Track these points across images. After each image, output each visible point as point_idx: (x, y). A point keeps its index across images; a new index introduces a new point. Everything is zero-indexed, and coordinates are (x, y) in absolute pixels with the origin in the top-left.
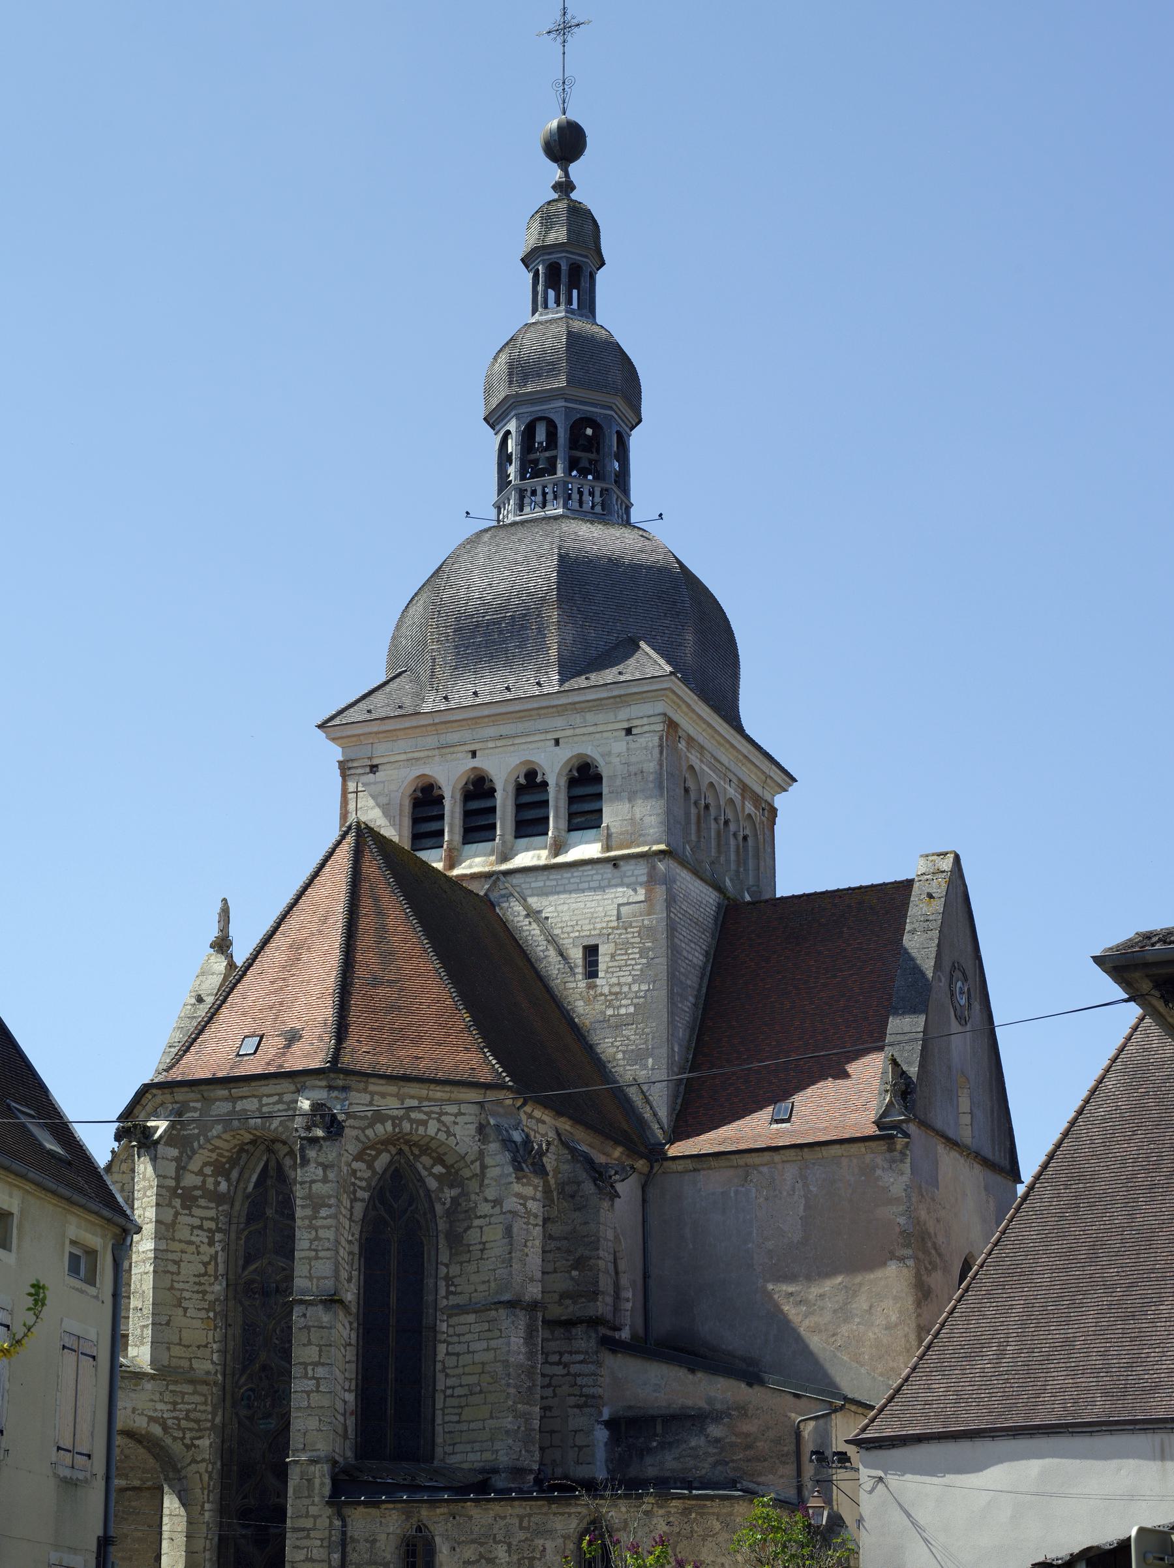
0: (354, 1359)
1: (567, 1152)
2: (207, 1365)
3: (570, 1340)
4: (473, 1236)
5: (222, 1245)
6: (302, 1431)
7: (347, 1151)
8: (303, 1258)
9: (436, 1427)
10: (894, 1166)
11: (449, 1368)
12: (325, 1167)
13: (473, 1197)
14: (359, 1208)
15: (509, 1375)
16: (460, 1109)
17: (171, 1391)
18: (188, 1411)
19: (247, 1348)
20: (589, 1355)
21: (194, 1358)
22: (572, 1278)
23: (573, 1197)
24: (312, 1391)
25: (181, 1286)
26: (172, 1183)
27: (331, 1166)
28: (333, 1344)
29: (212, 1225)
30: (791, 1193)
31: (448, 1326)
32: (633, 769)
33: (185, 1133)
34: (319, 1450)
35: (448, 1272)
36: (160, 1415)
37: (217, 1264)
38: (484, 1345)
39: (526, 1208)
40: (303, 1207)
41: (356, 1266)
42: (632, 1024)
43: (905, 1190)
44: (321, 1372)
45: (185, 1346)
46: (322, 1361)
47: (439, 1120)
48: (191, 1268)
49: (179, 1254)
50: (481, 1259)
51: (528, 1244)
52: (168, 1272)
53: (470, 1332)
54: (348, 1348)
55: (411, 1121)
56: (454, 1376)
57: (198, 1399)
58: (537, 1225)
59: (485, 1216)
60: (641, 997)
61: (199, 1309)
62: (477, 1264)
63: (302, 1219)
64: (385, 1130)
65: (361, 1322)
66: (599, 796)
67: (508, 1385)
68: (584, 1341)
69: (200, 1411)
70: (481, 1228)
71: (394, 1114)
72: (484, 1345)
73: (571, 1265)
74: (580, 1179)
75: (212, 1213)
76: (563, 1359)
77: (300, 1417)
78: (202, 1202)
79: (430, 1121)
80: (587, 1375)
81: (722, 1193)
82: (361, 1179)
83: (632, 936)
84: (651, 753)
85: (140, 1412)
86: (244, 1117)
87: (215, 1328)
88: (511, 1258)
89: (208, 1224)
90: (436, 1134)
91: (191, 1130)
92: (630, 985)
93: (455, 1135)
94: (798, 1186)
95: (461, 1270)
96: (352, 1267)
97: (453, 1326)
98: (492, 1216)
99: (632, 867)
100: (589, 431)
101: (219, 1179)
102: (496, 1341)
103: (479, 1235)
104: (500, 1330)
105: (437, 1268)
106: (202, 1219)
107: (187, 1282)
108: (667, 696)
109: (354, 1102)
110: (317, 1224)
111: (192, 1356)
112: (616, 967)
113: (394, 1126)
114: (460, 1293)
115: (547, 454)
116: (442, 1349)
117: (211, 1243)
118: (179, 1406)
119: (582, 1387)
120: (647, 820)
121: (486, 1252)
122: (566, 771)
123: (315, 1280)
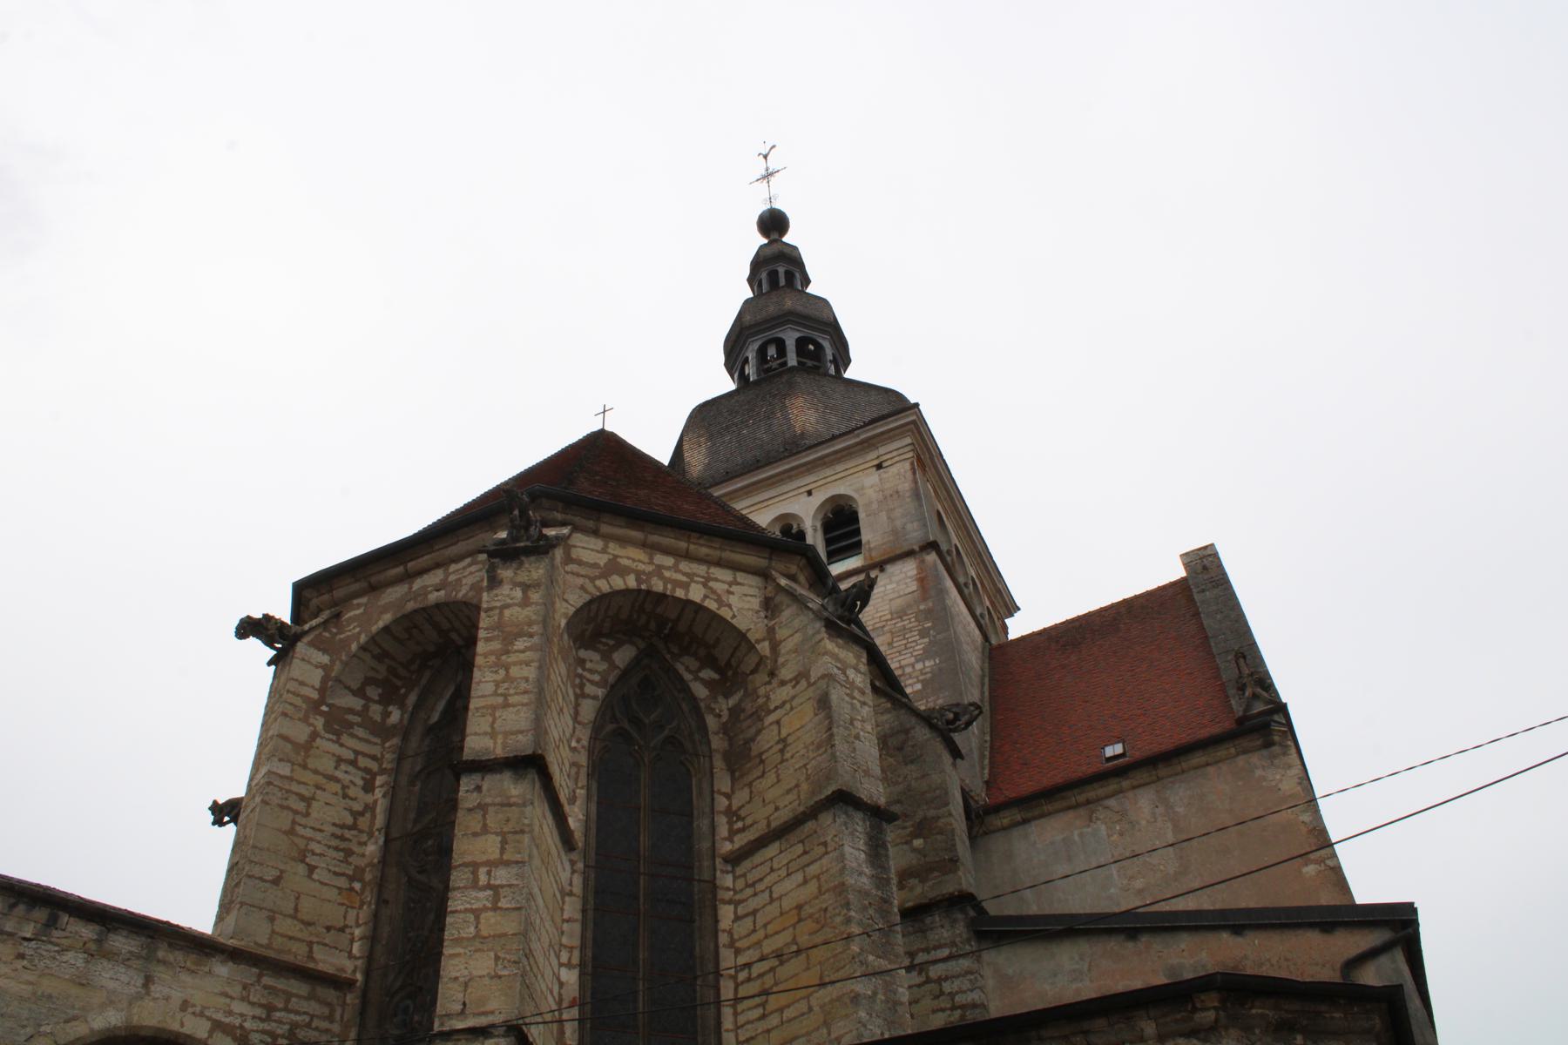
0: (578, 916)
1: (883, 700)
2: (344, 959)
3: (923, 931)
4: (767, 740)
5: (383, 790)
6: (461, 979)
7: (566, 601)
8: (483, 707)
9: (725, 1035)
10: (1276, 762)
11: (740, 939)
12: (526, 588)
13: (762, 691)
14: (588, 710)
15: (847, 905)
16: (735, 578)
17: (265, 987)
18: (294, 1026)
19: (411, 935)
20: (956, 946)
21: (318, 943)
22: (914, 850)
23: (900, 749)
24: (485, 909)
25: (308, 833)
26: (315, 695)
27: (537, 585)
28: (527, 829)
29: (374, 766)
30: (1153, 820)
31: (735, 879)
32: (888, 493)
33: (342, 636)
34: (492, 1012)
35: (730, 805)
36: (237, 1022)
37: (374, 817)
38: (799, 877)
39: (848, 677)
40: (487, 640)
41: (583, 781)
42: (922, 699)
43: (1300, 784)
44: (502, 876)
45: (303, 922)
46: (505, 857)
47: (705, 585)
48: (328, 812)
49: (312, 790)
50: (783, 761)
51: (855, 723)
52: (288, 808)
53: (772, 870)
54: (567, 899)
55: (666, 581)
56: (749, 948)
57: (314, 1007)
58: (864, 703)
59: (784, 703)
60: (926, 673)
61: (335, 873)
62: (776, 772)
63: (485, 655)
64: (625, 584)
65: (592, 863)
66: (857, 532)
67: (848, 921)
68: (948, 931)
69: (316, 1029)
70: (778, 722)
71: (639, 568)
72: (799, 877)
73: (911, 832)
74: (908, 726)
75: (376, 751)
76: (916, 962)
77: (458, 955)
78: (360, 732)
79: (693, 585)
80: (957, 977)
81: (1064, 839)
82: (591, 671)
83: (909, 622)
84: (905, 477)
85: (198, 1009)
86: (424, 592)
87: (362, 904)
88: (832, 735)
89: (363, 762)
90: (703, 600)
91: (350, 631)
92: (913, 665)
93: (730, 606)
94: (1161, 810)
95: (751, 792)
96: (576, 784)
97: (744, 875)
98: (793, 698)
99: (900, 567)
100: (811, 347)
101: (391, 708)
102: (819, 862)
103: (776, 732)
104: (825, 844)
105: (713, 799)
106: (357, 753)
107: (321, 831)
108: (913, 432)
109: (578, 544)
110: (509, 660)
111: (315, 940)
112: (895, 653)
113: (638, 580)
114: (751, 825)
115: (778, 362)
116: (726, 913)
117: (368, 787)
118: (278, 1014)
119: (952, 995)
120: (909, 527)
121: (788, 748)
122: (820, 516)
123: (500, 737)
